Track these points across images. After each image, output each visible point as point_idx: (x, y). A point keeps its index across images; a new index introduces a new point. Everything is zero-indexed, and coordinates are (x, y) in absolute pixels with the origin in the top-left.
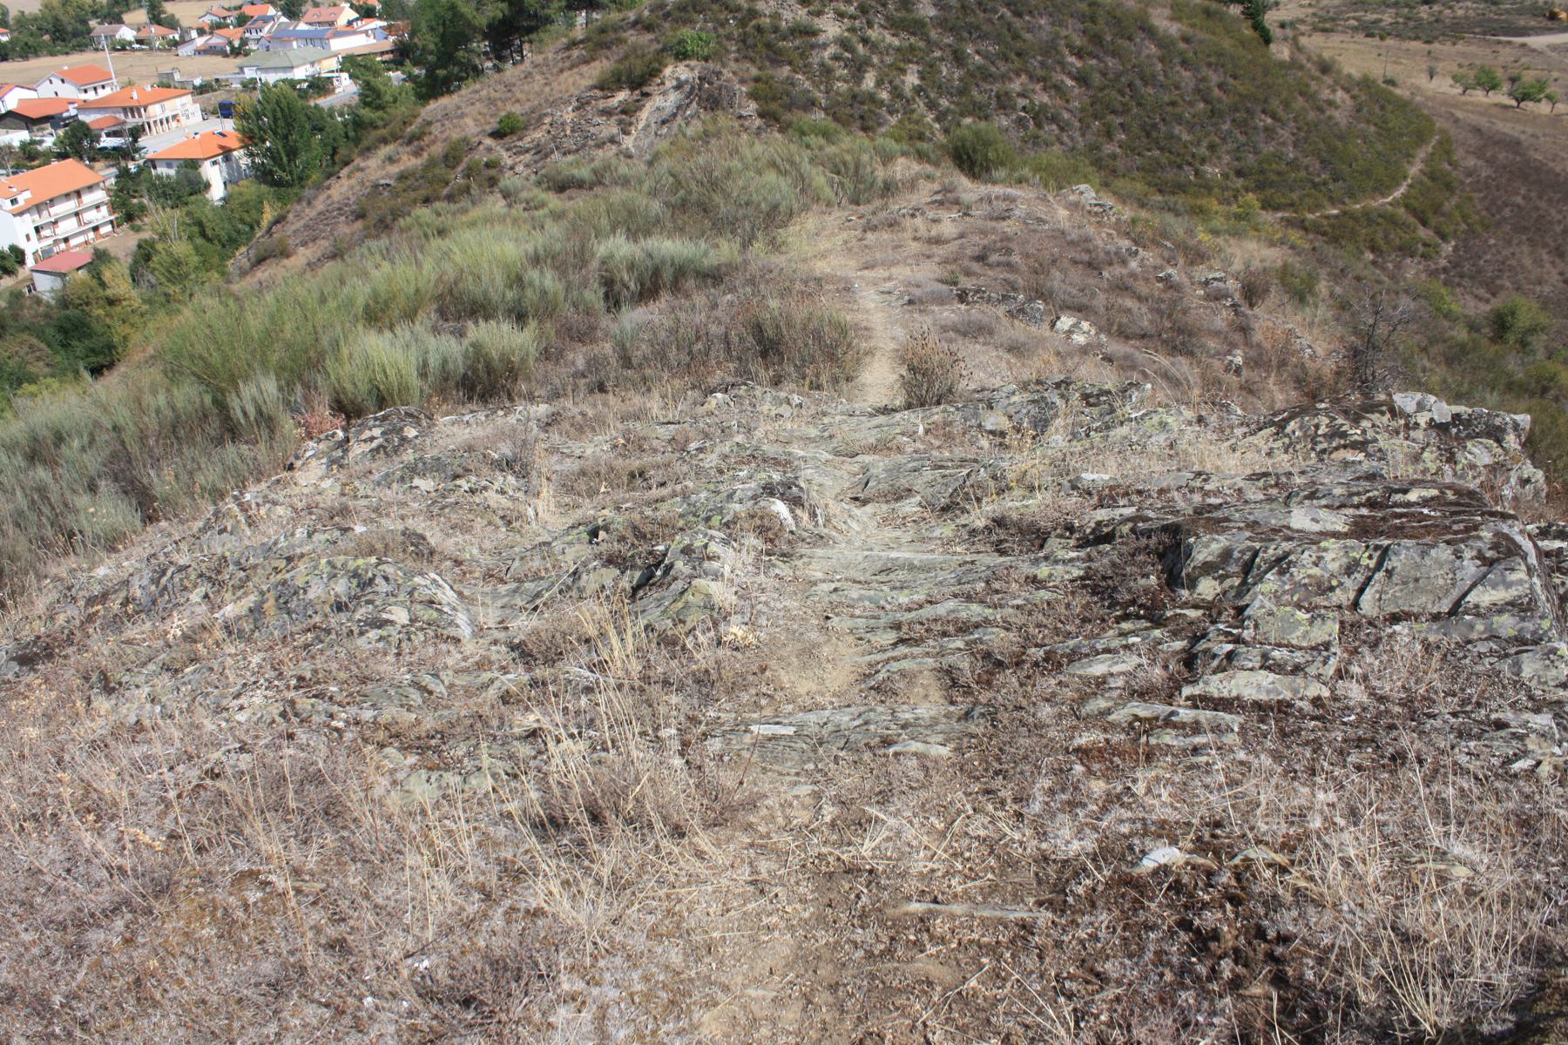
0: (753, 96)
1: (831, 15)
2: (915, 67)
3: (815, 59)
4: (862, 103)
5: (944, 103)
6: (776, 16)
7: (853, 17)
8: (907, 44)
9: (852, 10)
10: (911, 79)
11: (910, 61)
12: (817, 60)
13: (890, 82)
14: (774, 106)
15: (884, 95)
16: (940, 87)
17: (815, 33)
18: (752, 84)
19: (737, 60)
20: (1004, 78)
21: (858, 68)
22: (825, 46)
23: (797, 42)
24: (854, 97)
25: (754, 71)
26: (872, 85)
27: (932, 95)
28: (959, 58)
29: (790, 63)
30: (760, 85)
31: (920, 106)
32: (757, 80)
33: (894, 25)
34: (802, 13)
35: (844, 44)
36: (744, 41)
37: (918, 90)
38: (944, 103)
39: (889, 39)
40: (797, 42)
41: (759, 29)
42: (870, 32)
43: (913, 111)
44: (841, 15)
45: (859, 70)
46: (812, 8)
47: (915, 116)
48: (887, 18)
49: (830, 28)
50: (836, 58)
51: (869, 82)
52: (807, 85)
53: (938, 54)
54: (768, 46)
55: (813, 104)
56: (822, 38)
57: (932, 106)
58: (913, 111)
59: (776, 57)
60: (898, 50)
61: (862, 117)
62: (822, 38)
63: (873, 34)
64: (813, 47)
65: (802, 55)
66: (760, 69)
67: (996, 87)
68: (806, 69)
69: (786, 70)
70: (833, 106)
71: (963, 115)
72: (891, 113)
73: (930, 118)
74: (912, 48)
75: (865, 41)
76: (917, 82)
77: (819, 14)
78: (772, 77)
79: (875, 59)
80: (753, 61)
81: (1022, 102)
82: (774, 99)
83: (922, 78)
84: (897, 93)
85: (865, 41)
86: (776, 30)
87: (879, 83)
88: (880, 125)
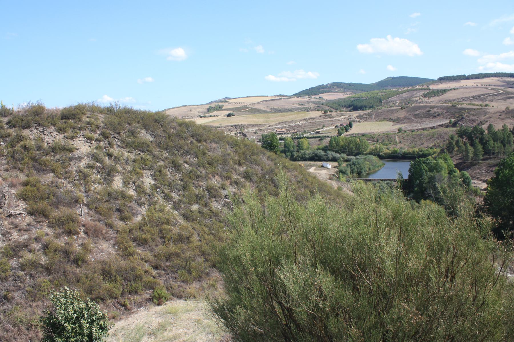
0: (23, 197)
1: (82, 139)
2: (149, 173)
3: (73, 167)
4: (116, 199)
5: (175, 195)
6: (39, 139)
7: (97, 140)
8: (139, 158)
9: (96, 136)
10: (148, 181)
11: (144, 169)
12: (75, 169)
13: (134, 183)
14: (42, 205)
15: (131, 192)
16: (169, 186)
17: (71, 150)
18: (21, 188)
19: (7, 170)
20: (207, 177)
21: (109, 174)
22: (80, 159)
23: (58, 157)
24: (109, 194)
25: (22, 177)
26: (121, 185)
27: (166, 191)
28: (176, 166)
29: (53, 171)
30: (29, 188)
31: (159, 199)
32: (25, 184)
33: (127, 145)
34: (60, 138)
35: (95, 157)
36: (13, 157)
37: (155, 188)
38: (175, 195)
39: (126, 154)
40: (58, 157)
41: (25, 148)
42: (111, 150)
43: (156, 203)
44: (89, 139)
45: (109, 175)
46: (66, 134)
47: (157, 206)
48: (122, 142)
49: (82, 147)
50: (90, 167)
51: (118, 183)
52: (69, 186)
53: (162, 163)
54: (34, 159)
55: (77, 201)
56: (77, 153)
57: (167, 198)
58: (156, 203)
59: (42, 167)
60: (134, 161)
61: (119, 210)
62: (77, 153)
63: (115, 151)
64: (71, 159)
65: (63, 166)
66: (28, 176)
67: (204, 184)
68: (67, 175)
69: (50, 177)
70: (94, 202)
71: (190, 204)
72: (140, 205)
73: (169, 207)
74: (144, 160)
75: (110, 155)
76: (153, 182)
77: (72, 138)
78: (40, 182)
79: (119, 168)
80: (21, 170)
81: (224, 193)
82: (42, 198)
83: (155, 180)
84: (140, 189)
85: (110, 155)
86: (39, 148)
87: (126, 183)
88: (134, 215)
